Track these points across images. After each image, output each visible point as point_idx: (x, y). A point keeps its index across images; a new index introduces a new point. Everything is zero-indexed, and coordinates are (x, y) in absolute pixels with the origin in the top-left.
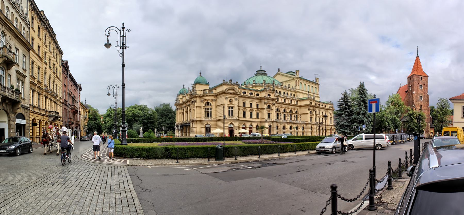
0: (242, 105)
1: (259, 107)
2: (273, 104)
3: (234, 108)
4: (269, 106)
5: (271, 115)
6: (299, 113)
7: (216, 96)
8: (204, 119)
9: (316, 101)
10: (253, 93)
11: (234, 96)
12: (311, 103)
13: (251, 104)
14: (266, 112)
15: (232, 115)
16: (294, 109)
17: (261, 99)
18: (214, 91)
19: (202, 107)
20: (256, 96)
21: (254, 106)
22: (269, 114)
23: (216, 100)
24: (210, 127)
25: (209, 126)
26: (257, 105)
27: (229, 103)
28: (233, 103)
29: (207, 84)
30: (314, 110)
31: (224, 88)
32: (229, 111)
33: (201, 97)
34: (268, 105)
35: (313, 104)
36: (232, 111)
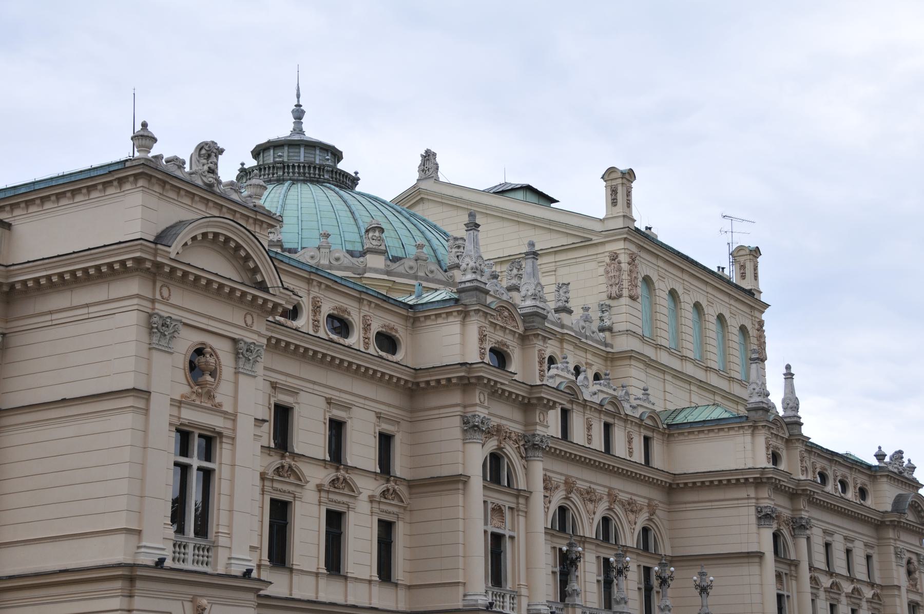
1: (399, 467)
2: (531, 446)
3: (223, 452)
4: (495, 460)
6: (666, 549)
11: (229, 319)
13: (337, 428)
15: (202, 530)
16: (631, 507)
17: (417, 388)
20: (373, 349)
21: (361, 450)
22: (497, 541)
26: (385, 441)
27: (182, 388)
28: (223, 393)
34: (492, 445)
35: (793, 465)
36: (207, 475)
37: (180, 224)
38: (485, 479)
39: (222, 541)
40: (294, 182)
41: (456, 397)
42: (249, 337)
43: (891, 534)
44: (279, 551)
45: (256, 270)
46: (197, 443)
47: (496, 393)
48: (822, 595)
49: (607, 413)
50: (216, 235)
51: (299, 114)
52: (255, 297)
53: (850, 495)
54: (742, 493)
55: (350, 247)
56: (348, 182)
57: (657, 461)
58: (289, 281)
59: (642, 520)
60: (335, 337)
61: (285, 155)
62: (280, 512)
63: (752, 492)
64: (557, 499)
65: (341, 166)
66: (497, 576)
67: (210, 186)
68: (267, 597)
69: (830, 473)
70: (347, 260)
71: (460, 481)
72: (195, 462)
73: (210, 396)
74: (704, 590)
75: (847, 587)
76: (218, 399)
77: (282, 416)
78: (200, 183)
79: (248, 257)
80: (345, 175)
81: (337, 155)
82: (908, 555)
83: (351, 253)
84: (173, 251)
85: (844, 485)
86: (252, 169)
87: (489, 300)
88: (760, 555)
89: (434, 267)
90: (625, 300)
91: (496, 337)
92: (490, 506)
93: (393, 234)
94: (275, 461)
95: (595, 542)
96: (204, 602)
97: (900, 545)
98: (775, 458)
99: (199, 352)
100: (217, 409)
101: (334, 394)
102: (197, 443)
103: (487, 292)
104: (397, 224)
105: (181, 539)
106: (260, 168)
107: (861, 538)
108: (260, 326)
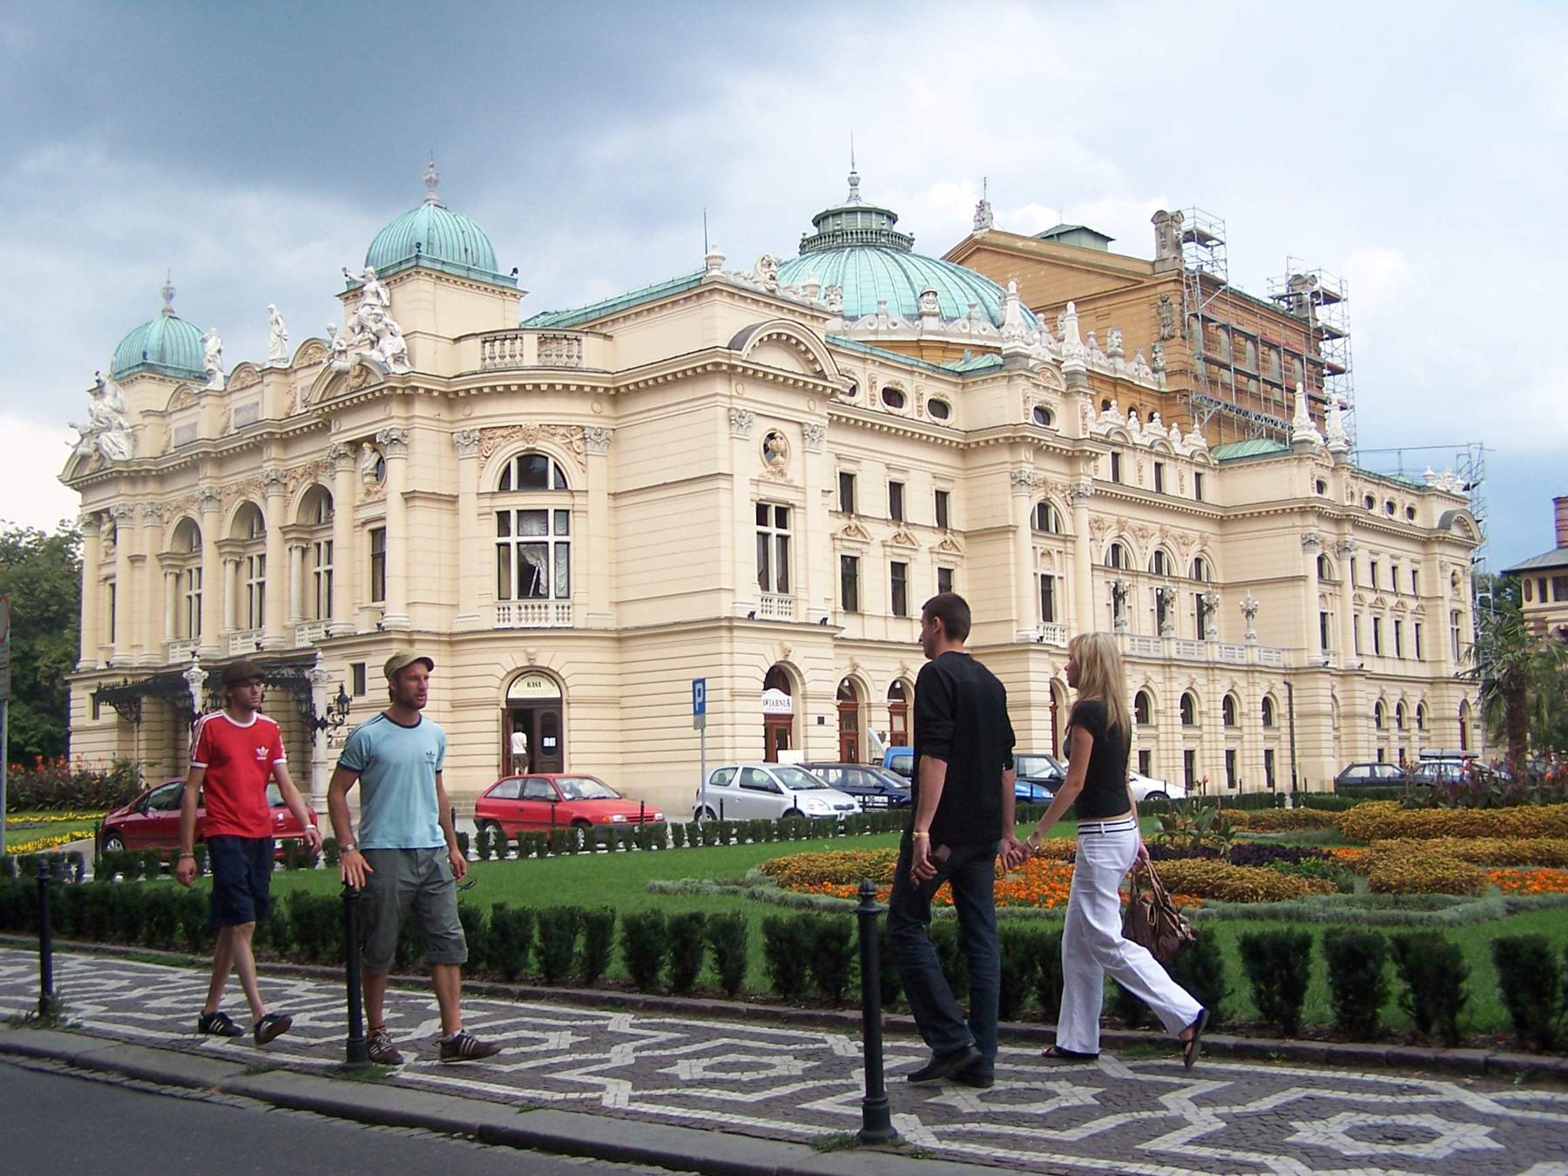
0: (835, 501)
1: (956, 519)
4: (1043, 508)
5: (1057, 586)
6: (1218, 577)
7: (617, 394)
8: (489, 620)
9: (1356, 474)
10: (908, 385)
11: (797, 406)
12: (1321, 486)
13: (896, 489)
14: (1024, 557)
15: (784, 586)
17: (968, 448)
18: (593, 353)
19: (469, 504)
21: (919, 507)
22: (1047, 580)
23: (610, 439)
24: (559, 701)
25: (547, 691)
26: (941, 497)
29: (505, 286)
30: (1343, 549)
31: (720, 323)
32: (764, 537)
33: (452, 399)
34: (1039, 496)
36: (784, 539)
37: (749, 330)
38: (1033, 527)
39: (801, 595)
40: (853, 248)
41: (1005, 456)
42: (812, 420)
43: (1437, 549)
44: (850, 601)
45: (815, 360)
46: (773, 515)
47: (1040, 449)
48: (1366, 609)
49: (1158, 454)
50: (779, 335)
51: (854, 184)
52: (815, 385)
53: (1399, 515)
54: (1288, 522)
55: (906, 311)
56: (902, 244)
57: (1208, 496)
58: (843, 363)
59: (1194, 552)
60: (891, 408)
61: (844, 222)
62: (850, 567)
63: (1298, 521)
64: (1109, 539)
65: (897, 228)
66: (1048, 615)
67: (772, 291)
68: (843, 639)
69: (1377, 496)
70: (903, 324)
71: (1008, 530)
72: (773, 529)
73: (782, 473)
74: (1249, 613)
75: (1391, 601)
76: (789, 477)
77: (847, 480)
78: (763, 290)
79: (808, 350)
80: (901, 237)
81: (893, 218)
82: (1453, 568)
83: (909, 317)
84: (744, 353)
85: (1391, 507)
86: (813, 240)
87: (1031, 363)
88: (1303, 578)
89: (989, 325)
90: (1178, 340)
91: (1039, 397)
92: (1040, 551)
93: (947, 295)
94: (843, 522)
95: (1149, 575)
96: (788, 645)
97: (1445, 559)
98: (1321, 486)
99: (771, 436)
100: (789, 485)
101: (894, 461)
102: (773, 515)
103: (1028, 357)
104: (950, 284)
105: (766, 595)
106: (820, 237)
107: (1407, 555)
108: (823, 410)
